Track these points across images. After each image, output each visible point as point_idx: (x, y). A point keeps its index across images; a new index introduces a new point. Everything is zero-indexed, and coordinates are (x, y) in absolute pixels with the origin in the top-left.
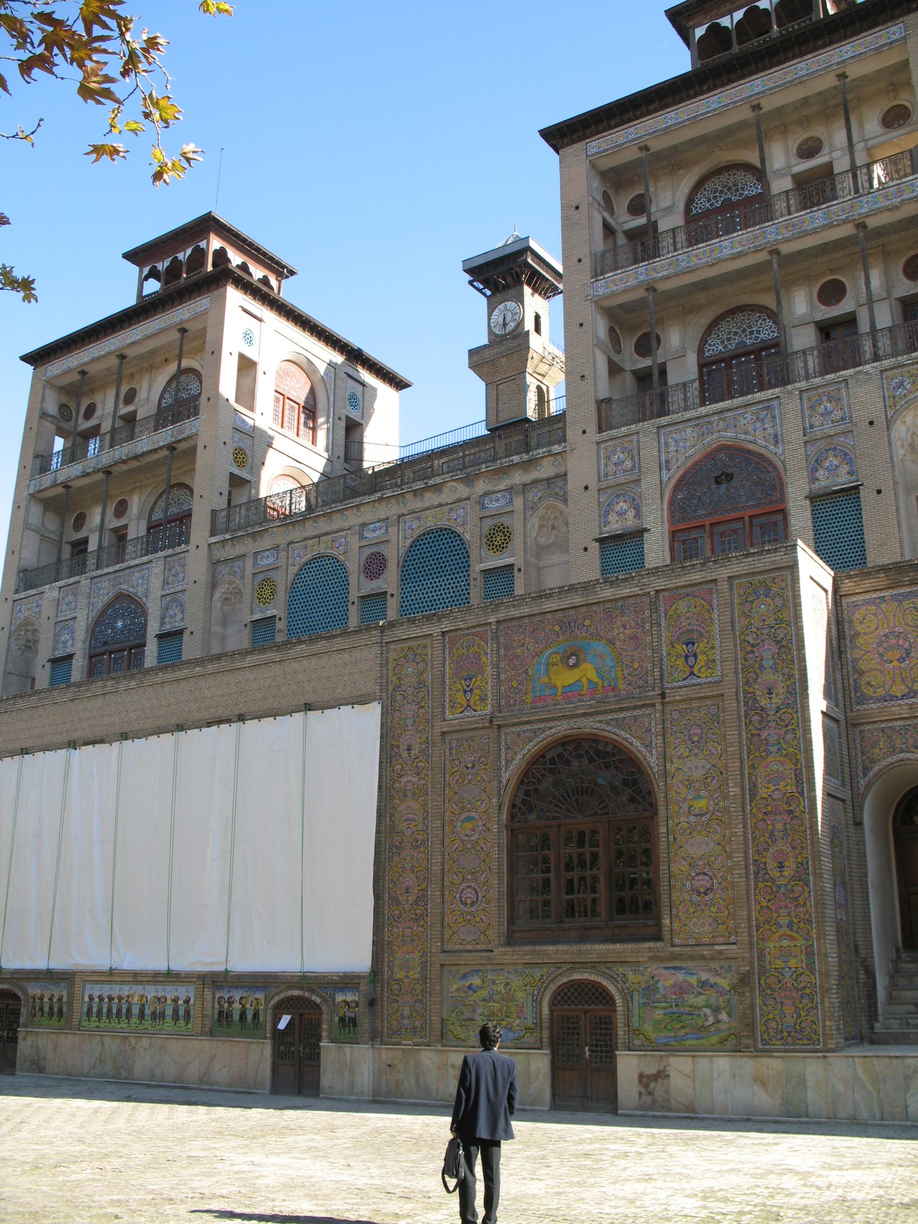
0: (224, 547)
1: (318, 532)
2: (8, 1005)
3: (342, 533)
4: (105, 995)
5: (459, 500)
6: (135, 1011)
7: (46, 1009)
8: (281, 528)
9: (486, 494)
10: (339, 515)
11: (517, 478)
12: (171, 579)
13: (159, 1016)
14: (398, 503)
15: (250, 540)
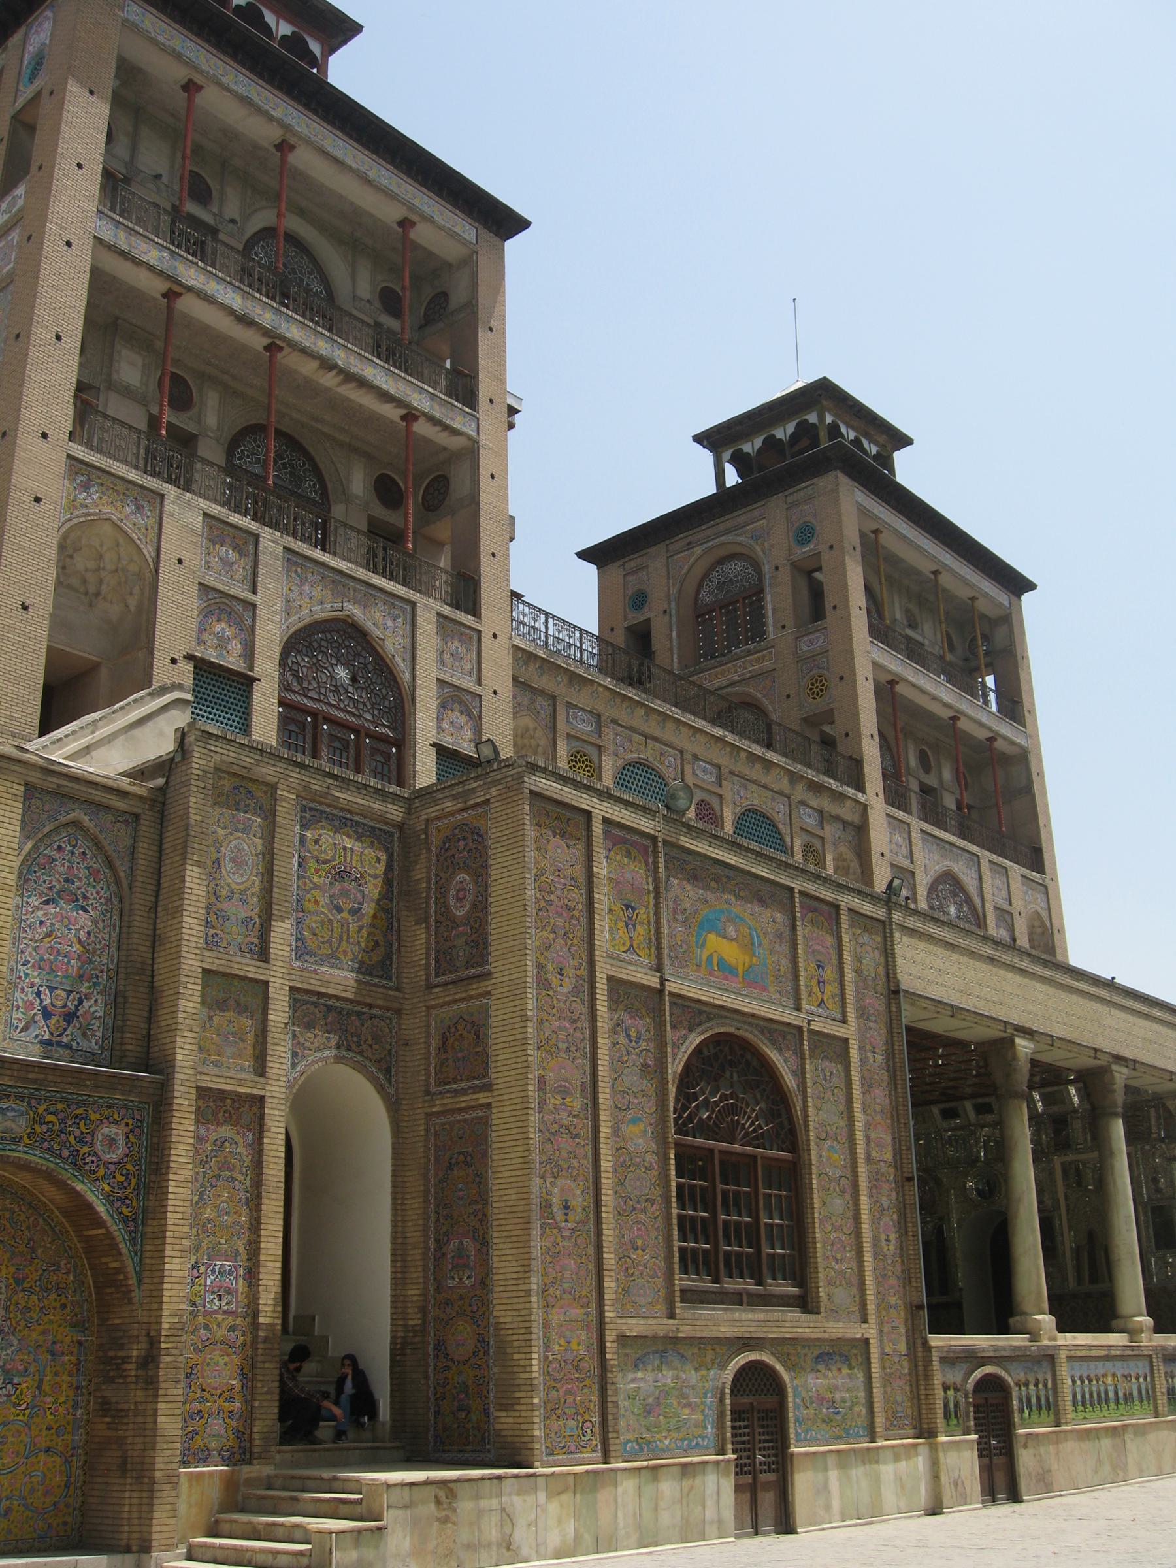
0: (526, 663)
1: (648, 731)
2: (986, 1399)
3: (673, 752)
4: (1085, 1375)
5: (781, 793)
6: (1111, 1394)
7: (1034, 1400)
8: (607, 693)
9: (803, 803)
10: (674, 726)
11: (826, 804)
12: (447, 657)
13: (1128, 1398)
14: (731, 753)
15: (566, 678)
